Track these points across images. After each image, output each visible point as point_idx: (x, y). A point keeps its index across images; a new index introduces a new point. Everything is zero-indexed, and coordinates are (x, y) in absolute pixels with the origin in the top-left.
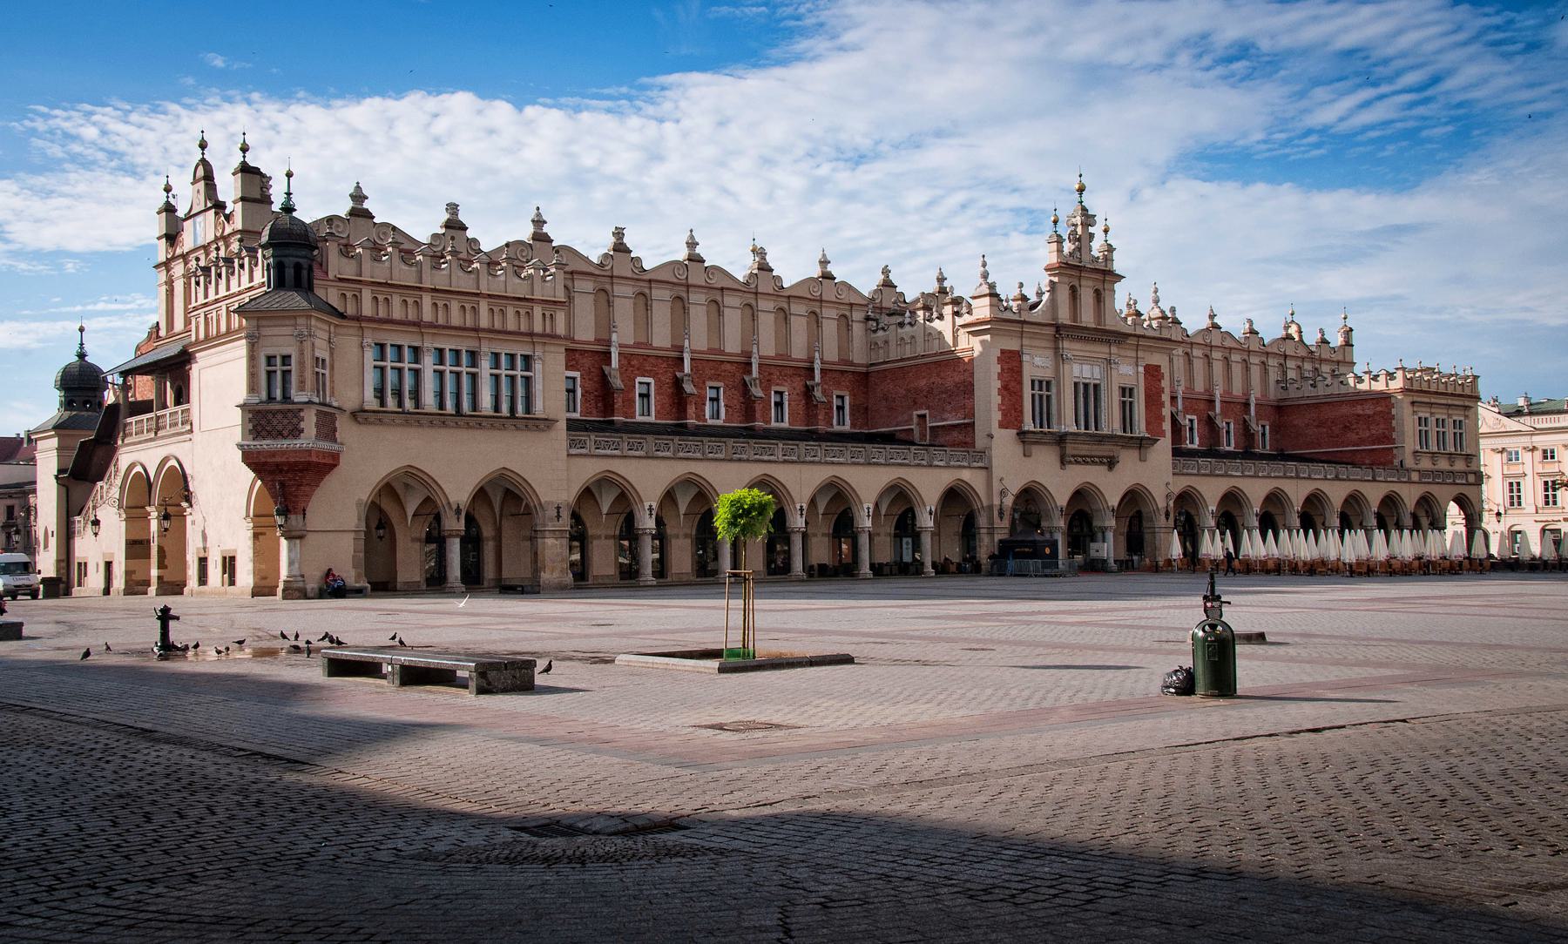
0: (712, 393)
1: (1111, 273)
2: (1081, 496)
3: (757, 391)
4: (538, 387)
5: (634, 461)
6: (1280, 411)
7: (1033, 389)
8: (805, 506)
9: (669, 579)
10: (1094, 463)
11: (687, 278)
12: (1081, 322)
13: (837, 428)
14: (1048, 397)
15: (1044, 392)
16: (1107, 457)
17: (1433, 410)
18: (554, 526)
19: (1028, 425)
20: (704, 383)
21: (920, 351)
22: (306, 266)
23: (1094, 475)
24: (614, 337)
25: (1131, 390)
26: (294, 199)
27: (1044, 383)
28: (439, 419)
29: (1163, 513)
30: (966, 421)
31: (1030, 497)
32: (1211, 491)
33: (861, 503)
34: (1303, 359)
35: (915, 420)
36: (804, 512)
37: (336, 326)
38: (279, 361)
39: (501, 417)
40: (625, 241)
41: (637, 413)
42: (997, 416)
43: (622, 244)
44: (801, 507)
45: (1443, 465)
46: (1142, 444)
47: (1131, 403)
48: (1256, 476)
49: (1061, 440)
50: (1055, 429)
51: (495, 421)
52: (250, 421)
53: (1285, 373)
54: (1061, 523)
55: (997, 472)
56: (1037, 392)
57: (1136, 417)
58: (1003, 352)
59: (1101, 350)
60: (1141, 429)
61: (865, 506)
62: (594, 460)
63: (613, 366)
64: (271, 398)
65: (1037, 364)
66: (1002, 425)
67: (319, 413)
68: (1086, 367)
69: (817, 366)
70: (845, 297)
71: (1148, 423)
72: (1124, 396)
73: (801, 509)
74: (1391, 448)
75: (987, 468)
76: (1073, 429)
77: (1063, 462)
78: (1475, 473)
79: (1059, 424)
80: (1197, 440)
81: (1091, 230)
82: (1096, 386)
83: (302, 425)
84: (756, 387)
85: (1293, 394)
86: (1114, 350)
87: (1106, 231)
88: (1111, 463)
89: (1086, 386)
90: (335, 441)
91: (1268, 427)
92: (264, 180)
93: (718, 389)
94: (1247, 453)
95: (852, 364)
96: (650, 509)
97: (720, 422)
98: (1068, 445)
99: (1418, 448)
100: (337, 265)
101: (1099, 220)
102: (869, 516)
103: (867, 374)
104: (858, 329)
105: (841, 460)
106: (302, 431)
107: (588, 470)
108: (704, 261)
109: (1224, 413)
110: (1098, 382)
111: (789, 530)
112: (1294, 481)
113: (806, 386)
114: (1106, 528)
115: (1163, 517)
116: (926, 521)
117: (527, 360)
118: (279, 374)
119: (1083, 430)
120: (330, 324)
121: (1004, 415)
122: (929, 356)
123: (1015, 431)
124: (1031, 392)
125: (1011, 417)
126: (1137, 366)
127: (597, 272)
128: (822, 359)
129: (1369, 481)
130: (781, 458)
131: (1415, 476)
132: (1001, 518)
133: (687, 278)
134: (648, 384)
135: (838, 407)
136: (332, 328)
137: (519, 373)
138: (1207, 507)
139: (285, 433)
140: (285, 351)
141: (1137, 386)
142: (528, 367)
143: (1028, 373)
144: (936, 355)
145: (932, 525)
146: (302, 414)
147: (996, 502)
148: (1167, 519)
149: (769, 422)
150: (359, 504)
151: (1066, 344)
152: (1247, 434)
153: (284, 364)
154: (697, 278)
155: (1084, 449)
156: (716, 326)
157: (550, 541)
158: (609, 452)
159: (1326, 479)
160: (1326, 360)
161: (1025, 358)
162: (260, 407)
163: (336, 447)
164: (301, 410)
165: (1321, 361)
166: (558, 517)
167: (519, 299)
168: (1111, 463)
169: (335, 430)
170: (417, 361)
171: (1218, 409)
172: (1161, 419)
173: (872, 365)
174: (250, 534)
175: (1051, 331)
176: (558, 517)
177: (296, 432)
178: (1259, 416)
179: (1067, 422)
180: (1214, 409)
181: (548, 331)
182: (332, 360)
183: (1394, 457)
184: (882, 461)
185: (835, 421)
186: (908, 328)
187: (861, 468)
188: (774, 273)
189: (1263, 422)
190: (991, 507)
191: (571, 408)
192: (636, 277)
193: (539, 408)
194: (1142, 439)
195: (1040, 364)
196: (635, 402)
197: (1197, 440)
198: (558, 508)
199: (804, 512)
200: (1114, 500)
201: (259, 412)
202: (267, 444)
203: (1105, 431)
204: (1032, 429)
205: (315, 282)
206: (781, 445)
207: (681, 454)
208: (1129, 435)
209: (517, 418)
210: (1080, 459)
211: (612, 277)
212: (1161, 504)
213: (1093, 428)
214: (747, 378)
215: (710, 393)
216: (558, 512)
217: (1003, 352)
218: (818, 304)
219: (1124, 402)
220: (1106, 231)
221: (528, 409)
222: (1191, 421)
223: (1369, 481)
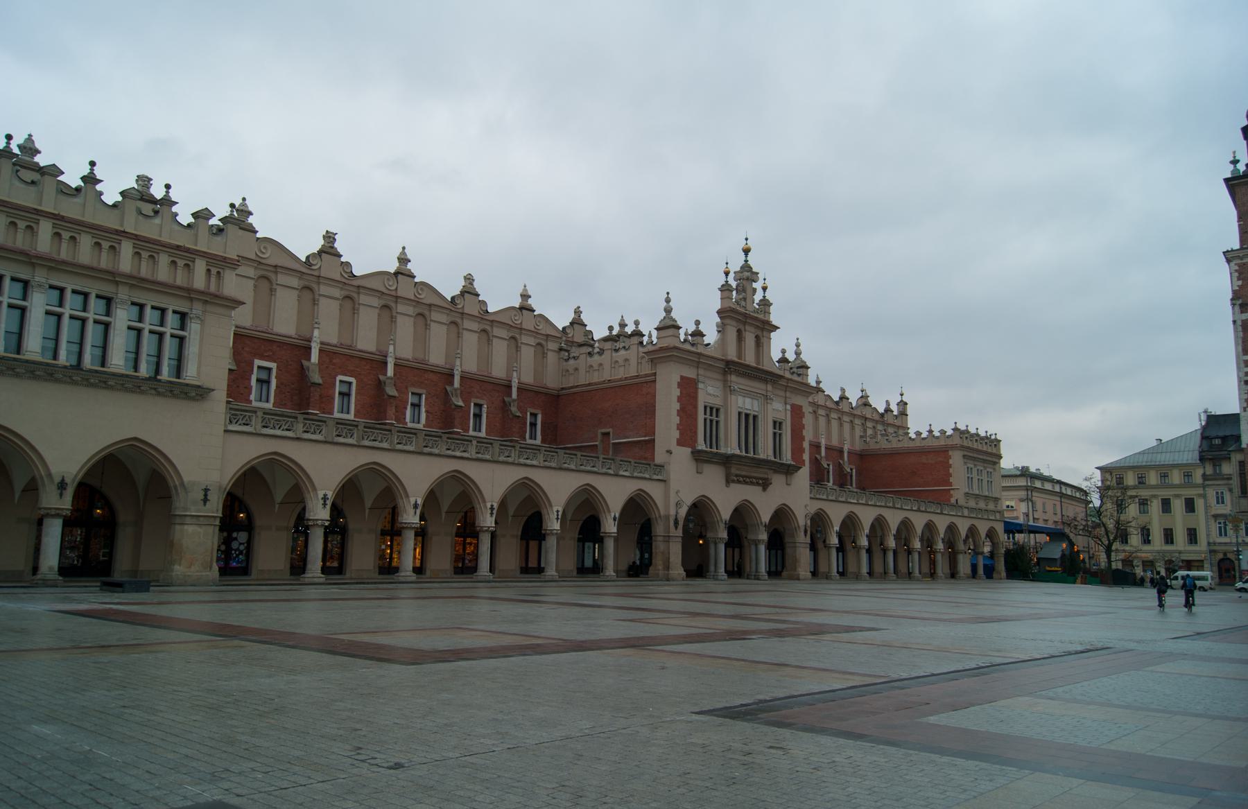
0: (411, 399)
1: (768, 323)
2: (742, 512)
4: (192, 349)
5: (308, 444)
6: (863, 458)
7: (705, 414)
8: (496, 506)
9: (348, 575)
10: (752, 483)
11: (396, 289)
12: (745, 360)
14: (717, 422)
15: (714, 417)
16: (761, 479)
17: (976, 463)
18: (198, 511)
19: (701, 445)
20: (407, 388)
21: (607, 376)
23: (751, 493)
24: (316, 333)
25: (780, 423)
27: (714, 410)
28: (44, 372)
29: (802, 529)
30: (647, 438)
31: (700, 510)
32: (837, 515)
33: (551, 506)
34: (877, 422)
35: (600, 436)
36: (495, 512)
40: (336, 245)
41: (336, 410)
43: (332, 247)
44: (492, 506)
45: (982, 505)
46: (788, 470)
47: (780, 434)
49: (726, 461)
50: (722, 451)
51: (128, 384)
53: (865, 431)
55: (674, 485)
56: (708, 416)
57: (784, 447)
58: (682, 378)
59: (758, 386)
60: (787, 458)
61: (555, 509)
62: (260, 439)
65: (709, 392)
66: (680, 443)
68: (748, 400)
70: (542, 328)
71: (793, 454)
73: (492, 508)
74: (950, 489)
75: (665, 481)
76: (737, 452)
77: (728, 481)
78: (999, 512)
79: (726, 446)
81: (755, 285)
82: (755, 417)
84: (457, 396)
85: (873, 446)
86: (770, 387)
87: (765, 289)
88: (765, 484)
89: (747, 416)
91: (854, 470)
93: (420, 395)
96: (325, 498)
99: (967, 490)
101: (761, 276)
102: (557, 519)
103: (558, 396)
104: (552, 358)
105: (534, 463)
107: (249, 450)
109: (827, 458)
110: (756, 414)
111: (478, 529)
113: (504, 401)
114: (759, 541)
115: (803, 533)
116: (610, 526)
117: (183, 316)
119: (744, 454)
122: (615, 381)
123: (690, 450)
124: (703, 416)
125: (687, 437)
126: (786, 404)
127: (304, 270)
128: (519, 379)
129: (938, 513)
130: (475, 456)
131: (966, 513)
132: (676, 528)
133: (396, 289)
134: (350, 384)
138: (833, 527)
143: (702, 399)
144: (621, 380)
145: (616, 531)
147: (673, 512)
148: (806, 535)
149: (468, 431)
151: (734, 378)
154: (405, 290)
156: (422, 339)
157: (190, 529)
158: (279, 432)
159: (912, 510)
160: (890, 424)
161: (701, 386)
165: (889, 425)
166: (205, 500)
167: (178, 247)
168: (765, 484)
171: (823, 453)
172: (803, 451)
173: (563, 389)
175: (722, 365)
176: (205, 500)
179: (731, 446)
180: (820, 453)
181: (213, 289)
183: (951, 496)
184: (573, 467)
185: (528, 435)
186: (596, 357)
187: (552, 472)
188: (480, 298)
189: (853, 467)
191: (264, 397)
192: (344, 280)
193: (191, 373)
194: (789, 466)
195: (712, 392)
196: (333, 399)
198: (206, 490)
199: (495, 512)
200: (766, 517)
203: (762, 456)
204: (704, 448)
207: (366, 443)
209: (160, 381)
210: (741, 479)
211: (319, 277)
213: (752, 453)
214: (448, 388)
215: (411, 399)
216: (206, 495)
217: (682, 378)
218: (518, 331)
219: (775, 434)
220: (765, 289)
221: (178, 370)
223: (938, 513)
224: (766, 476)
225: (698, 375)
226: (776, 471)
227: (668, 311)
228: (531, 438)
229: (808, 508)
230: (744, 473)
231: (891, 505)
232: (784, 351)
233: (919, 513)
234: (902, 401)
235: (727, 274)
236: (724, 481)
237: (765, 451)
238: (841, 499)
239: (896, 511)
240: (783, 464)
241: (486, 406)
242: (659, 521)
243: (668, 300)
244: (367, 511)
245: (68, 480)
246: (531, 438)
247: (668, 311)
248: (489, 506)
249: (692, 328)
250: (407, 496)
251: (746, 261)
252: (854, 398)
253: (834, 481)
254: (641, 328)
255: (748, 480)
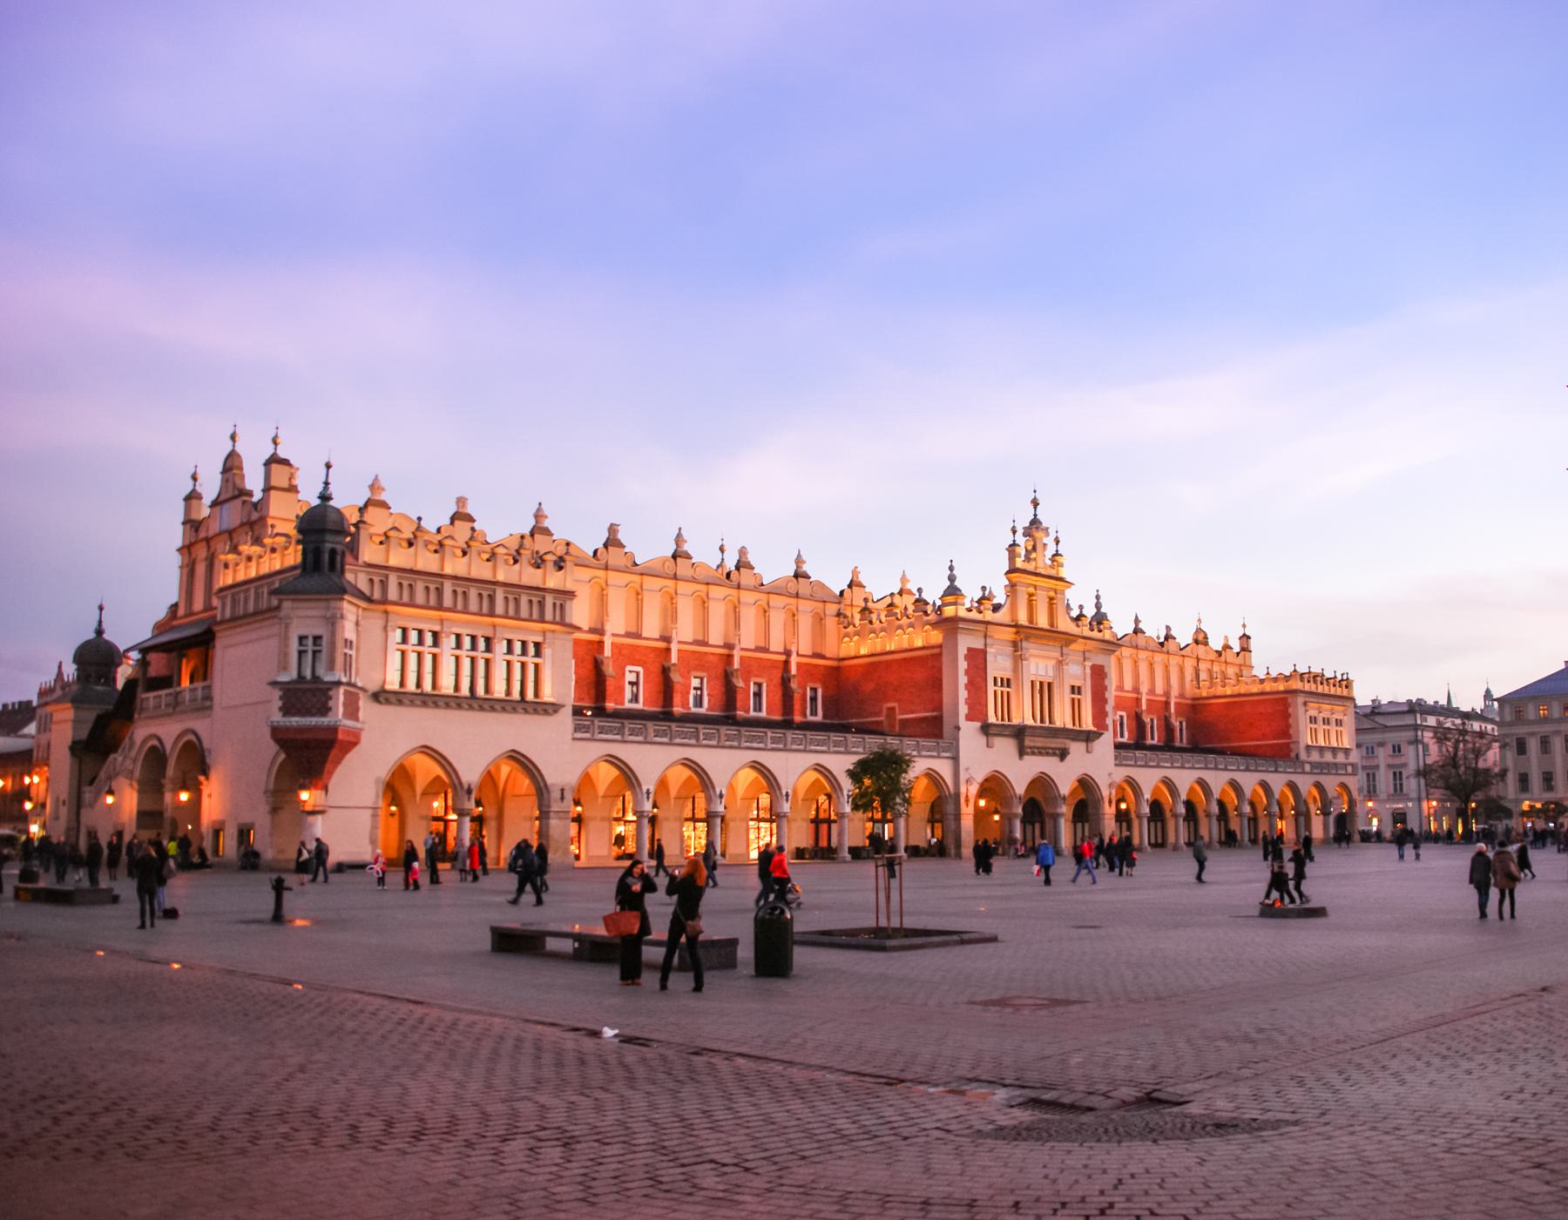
3: (739, 683)
6: (1195, 709)
7: (995, 684)
10: (1048, 754)
13: (811, 718)
16: (1059, 749)
20: (689, 672)
22: (339, 552)
23: (1046, 765)
25: (1079, 688)
26: (332, 488)
28: (453, 702)
31: (994, 786)
37: (364, 609)
38: (310, 641)
39: (512, 701)
42: (963, 709)
44: (787, 793)
46: (1088, 737)
48: (1182, 767)
49: (1019, 733)
52: (281, 698)
54: (1020, 810)
55: (964, 761)
58: (969, 650)
60: (1088, 724)
63: (606, 654)
64: (301, 677)
66: (969, 718)
67: (346, 692)
69: (794, 660)
72: (1073, 693)
77: (1022, 753)
80: (1126, 734)
82: (1049, 684)
83: (331, 703)
87: (1057, 541)
88: (1063, 754)
90: (357, 719)
91: (1184, 724)
92: (293, 471)
93: (702, 679)
94: (1168, 746)
95: (823, 657)
97: (702, 710)
98: (1027, 738)
100: (370, 552)
103: (837, 669)
106: (330, 709)
108: (691, 558)
109: (1149, 710)
112: (1214, 772)
117: (537, 645)
118: (310, 655)
119: (1038, 724)
120: (358, 606)
121: (970, 708)
123: (978, 724)
125: (977, 711)
130: (770, 746)
134: (638, 673)
135: (811, 699)
136: (360, 610)
137: (530, 660)
139: (314, 711)
140: (317, 632)
141: (1085, 684)
142: (538, 654)
146: (330, 693)
149: (748, 711)
150: (377, 781)
152: (1168, 729)
153: (315, 644)
155: (1040, 742)
159: (1239, 770)
162: (291, 686)
163: (359, 725)
164: (329, 689)
168: (1063, 754)
169: (357, 710)
170: (436, 644)
173: (844, 659)
174: (268, 808)
176: (562, 798)
177: (325, 710)
178: (1178, 713)
179: (1024, 714)
182: (358, 642)
188: (755, 571)
190: (957, 795)
194: (1089, 732)
197: (1126, 734)
198: (562, 790)
201: (289, 690)
202: (296, 721)
203: (1058, 724)
205: (347, 567)
206: (769, 734)
208: (1078, 728)
209: (527, 702)
212: (1105, 793)
217: (969, 650)
219: (1073, 700)
220: (1057, 541)
222: (1122, 717)
224: (1063, 746)
225: (986, 645)
226: (1074, 740)
227: (952, 579)
228: (812, 714)
229: (1113, 776)
230: (1039, 745)
231: (1213, 766)
232: (1081, 607)
233: (1248, 774)
234: (1244, 635)
235: (1014, 532)
236: (1017, 755)
237: (1062, 718)
238: (1152, 764)
239: (1218, 772)
240: (1082, 731)
241: (765, 685)
242: (949, 800)
243: (951, 568)
244: (672, 801)
245: (472, 787)
246: (812, 714)
247: (952, 579)
248: (784, 793)
249: (979, 595)
250: (713, 788)
251: (1035, 515)
252: (1184, 637)
253: (1159, 737)
254: (924, 596)
255: (1043, 751)
